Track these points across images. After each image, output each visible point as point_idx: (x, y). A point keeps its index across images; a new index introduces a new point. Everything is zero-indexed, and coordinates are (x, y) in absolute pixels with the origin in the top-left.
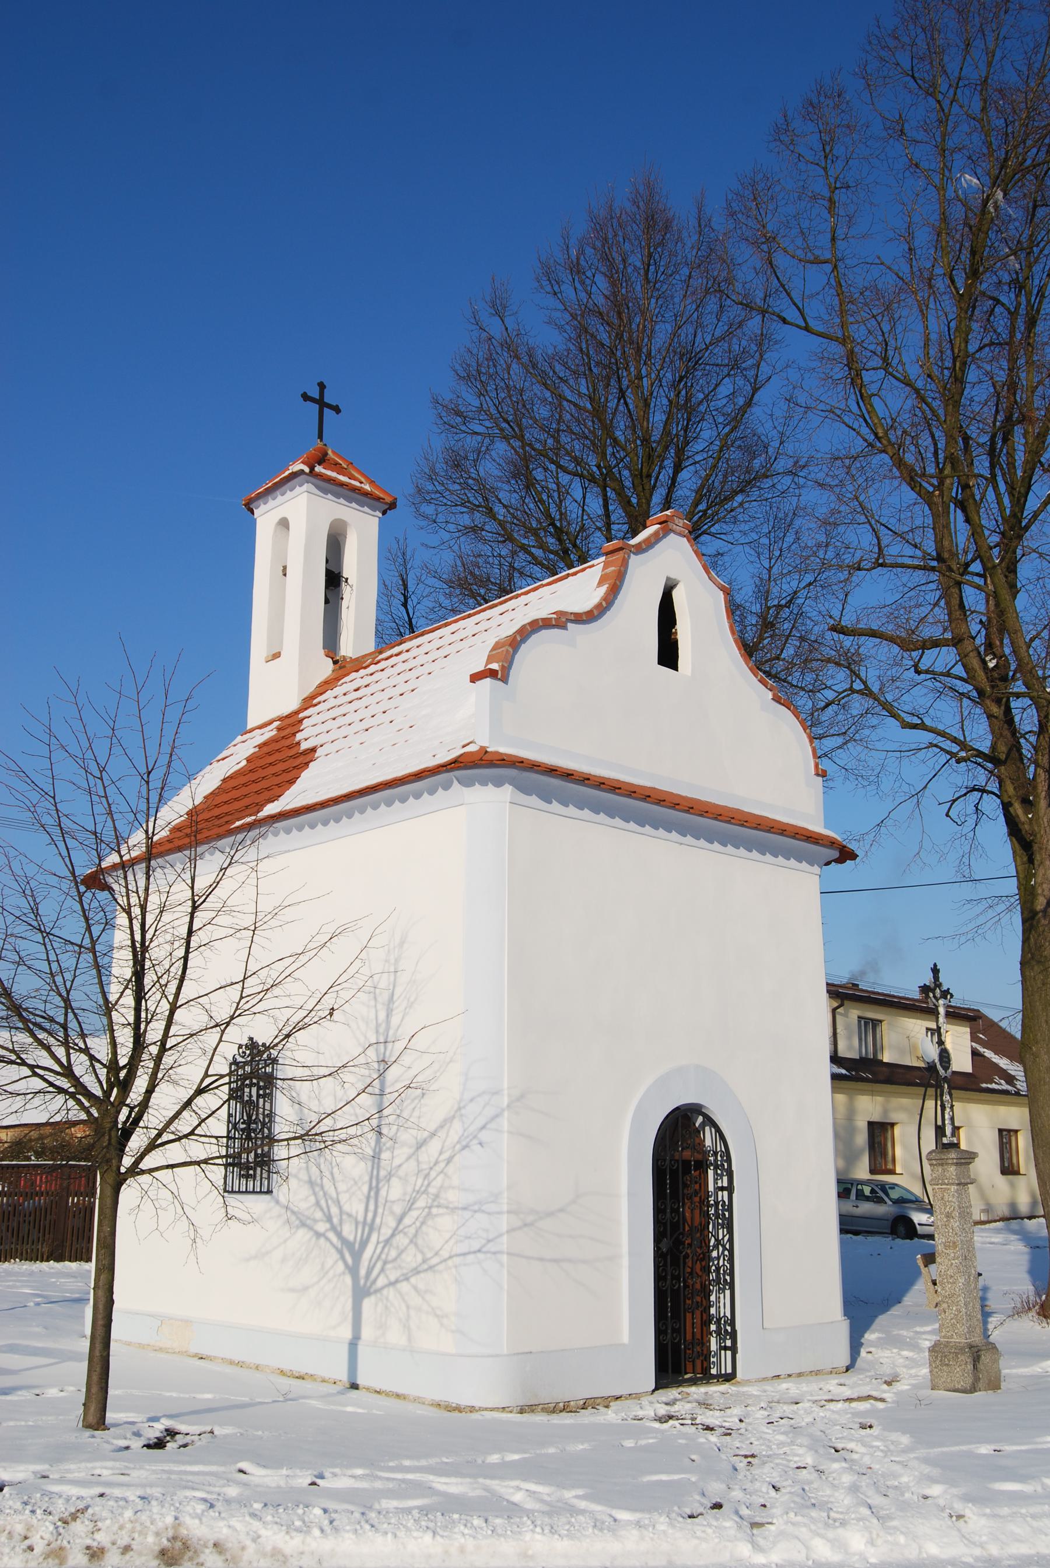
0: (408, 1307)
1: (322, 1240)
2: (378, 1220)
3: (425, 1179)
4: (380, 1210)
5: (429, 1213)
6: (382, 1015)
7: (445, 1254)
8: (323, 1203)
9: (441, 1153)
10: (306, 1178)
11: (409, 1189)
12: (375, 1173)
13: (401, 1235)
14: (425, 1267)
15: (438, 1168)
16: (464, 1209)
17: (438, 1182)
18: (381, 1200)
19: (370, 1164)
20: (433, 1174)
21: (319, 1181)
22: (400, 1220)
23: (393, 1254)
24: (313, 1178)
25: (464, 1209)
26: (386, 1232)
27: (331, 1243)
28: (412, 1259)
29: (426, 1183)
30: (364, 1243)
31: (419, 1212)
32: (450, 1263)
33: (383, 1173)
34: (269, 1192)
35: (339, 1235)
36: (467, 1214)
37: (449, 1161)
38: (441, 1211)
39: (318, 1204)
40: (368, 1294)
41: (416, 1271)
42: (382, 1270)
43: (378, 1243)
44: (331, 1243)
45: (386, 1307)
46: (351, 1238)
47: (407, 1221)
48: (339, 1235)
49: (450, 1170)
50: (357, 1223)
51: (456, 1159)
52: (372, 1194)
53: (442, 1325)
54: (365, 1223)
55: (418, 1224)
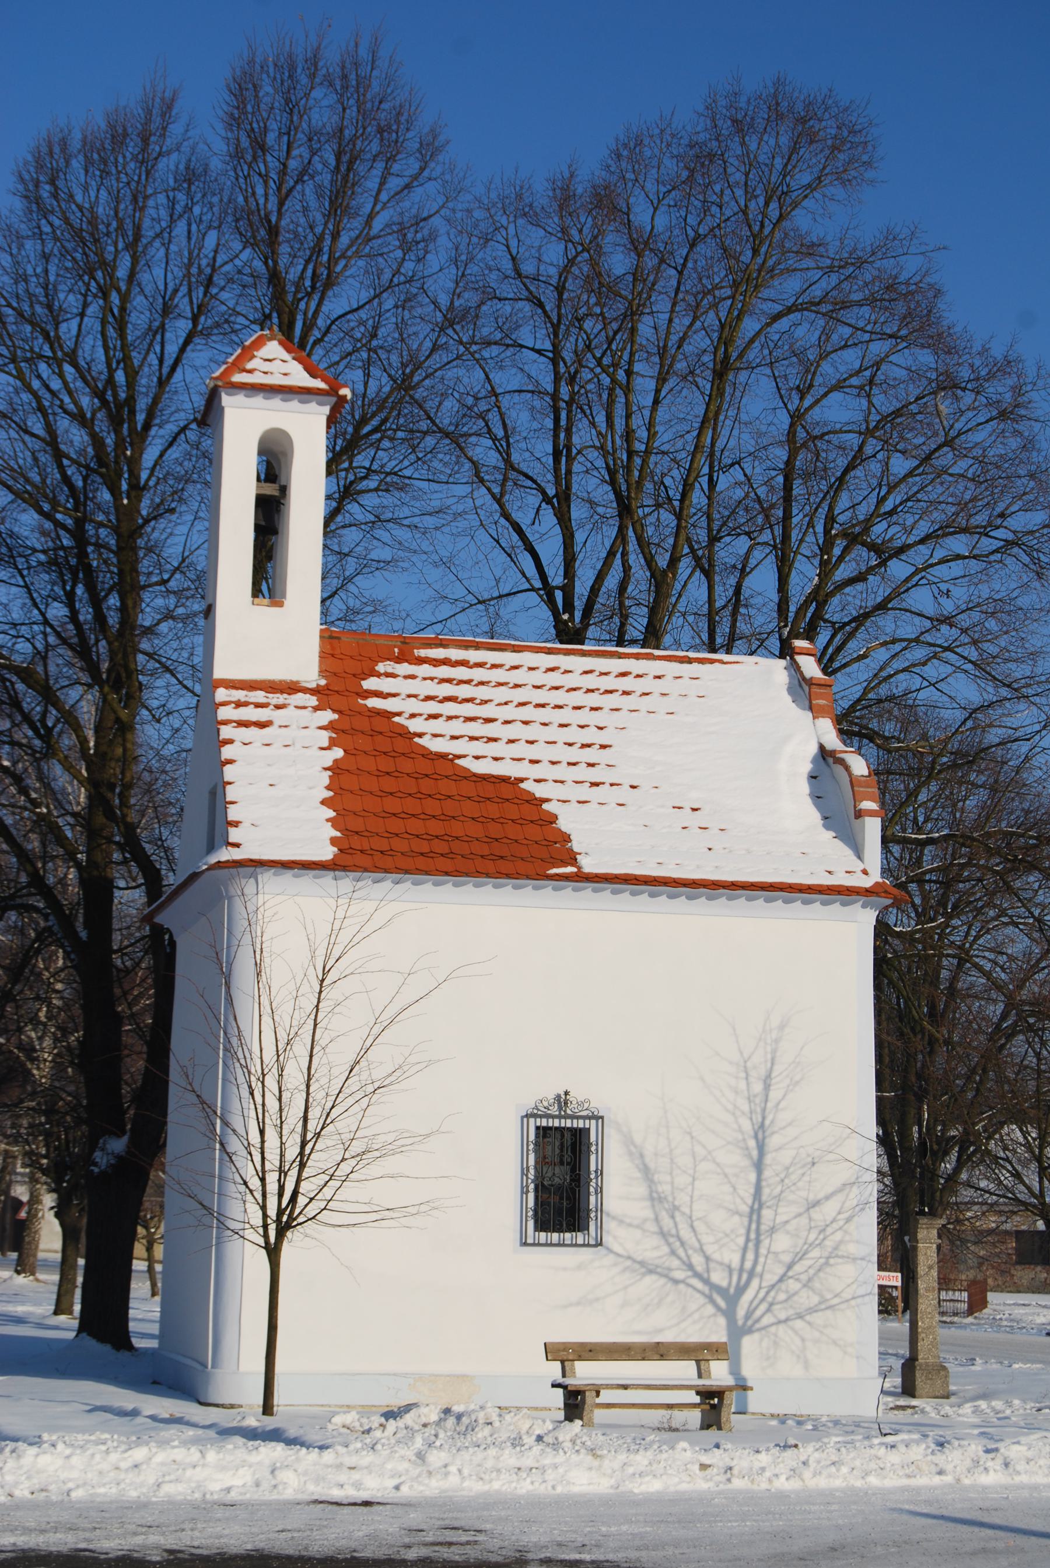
0: (803, 1340)
1: (682, 1286)
2: (759, 1269)
3: (820, 1232)
4: (762, 1260)
5: (827, 1263)
6: (758, 1087)
7: (846, 1295)
8: (681, 1252)
9: (839, 1213)
10: (655, 1229)
11: (801, 1242)
12: (754, 1226)
13: (791, 1281)
14: (824, 1306)
15: (835, 1226)
16: (862, 1259)
17: (838, 1236)
18: (763, 1251)
19: (746, 1221)
20: (829, 1230)
21: (674, 1232)
22: (790, 1267)
23: (782, 1296)
24: (665, 1229)
25: (862, 1259)
26: (770, 1279)
27: (699, 1291)
28: (806, 1299)
29: (821, 1237)
30: (741, 1290)
31: (811, 1262)
32: (853, 1302)
33: (763, 1228)
34: (599, 1244)
35: (706, 1281)
36: (864, 1263)
37: (848, 1220)
38: (840, 1260)
39: (673, 1253)
40: (750, 1331)
41: (812, 1310)
42: (768, 1310)
43: (760, 1288)
44: (699, 1291)
45: (775, 1343)
46: (724, 1284)
47: (798, 1268)
48: (706, 1281)
49: (851, 1227)
50: (730, 1270)
51: (856, 1219)
52: (751, 1245)
53: (845, 1353)
54: (741, 1270)
55: (811, 1272)
